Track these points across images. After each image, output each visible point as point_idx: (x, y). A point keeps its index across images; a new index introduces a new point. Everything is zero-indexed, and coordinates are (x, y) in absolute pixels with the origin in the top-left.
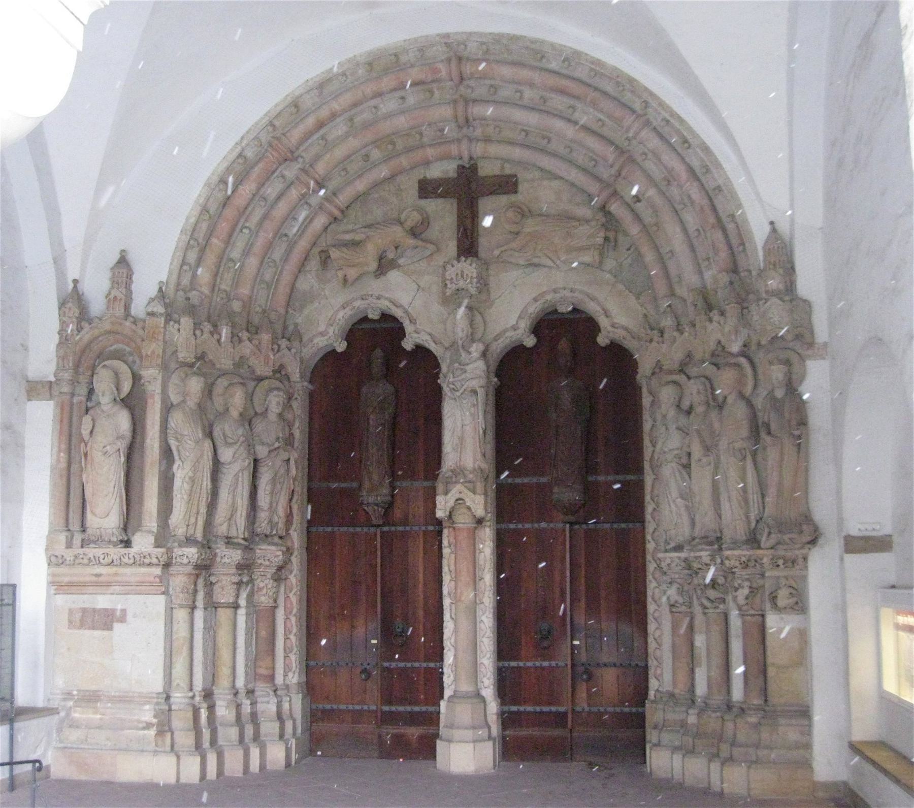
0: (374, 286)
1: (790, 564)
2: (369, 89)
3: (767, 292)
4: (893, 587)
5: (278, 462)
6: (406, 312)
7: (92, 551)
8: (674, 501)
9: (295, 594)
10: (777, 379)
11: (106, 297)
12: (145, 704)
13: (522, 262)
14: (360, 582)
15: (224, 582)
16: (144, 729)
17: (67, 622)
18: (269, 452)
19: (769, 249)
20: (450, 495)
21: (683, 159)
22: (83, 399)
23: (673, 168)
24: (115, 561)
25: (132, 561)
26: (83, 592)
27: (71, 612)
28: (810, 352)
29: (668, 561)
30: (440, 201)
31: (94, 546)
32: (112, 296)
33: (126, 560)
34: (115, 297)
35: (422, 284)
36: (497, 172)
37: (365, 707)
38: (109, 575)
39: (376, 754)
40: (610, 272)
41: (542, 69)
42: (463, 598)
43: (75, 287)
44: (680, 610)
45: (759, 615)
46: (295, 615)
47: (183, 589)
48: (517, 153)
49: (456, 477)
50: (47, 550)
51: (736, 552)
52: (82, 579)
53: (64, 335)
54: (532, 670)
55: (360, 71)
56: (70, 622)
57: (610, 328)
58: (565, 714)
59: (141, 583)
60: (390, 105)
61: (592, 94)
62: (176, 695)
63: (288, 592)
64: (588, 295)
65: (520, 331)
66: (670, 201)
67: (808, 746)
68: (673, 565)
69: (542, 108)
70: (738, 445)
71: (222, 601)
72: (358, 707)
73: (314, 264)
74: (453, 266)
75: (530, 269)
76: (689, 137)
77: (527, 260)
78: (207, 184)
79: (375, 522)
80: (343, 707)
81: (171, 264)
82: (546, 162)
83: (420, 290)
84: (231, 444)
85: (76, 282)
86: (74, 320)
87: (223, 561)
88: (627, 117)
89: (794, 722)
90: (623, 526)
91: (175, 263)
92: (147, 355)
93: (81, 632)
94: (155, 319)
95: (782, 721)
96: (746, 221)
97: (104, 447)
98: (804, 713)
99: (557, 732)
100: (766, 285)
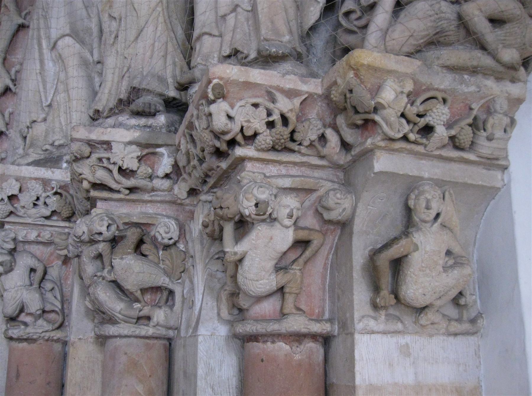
8: (54, 47)
45: (314, 337)
68: (26, 199)
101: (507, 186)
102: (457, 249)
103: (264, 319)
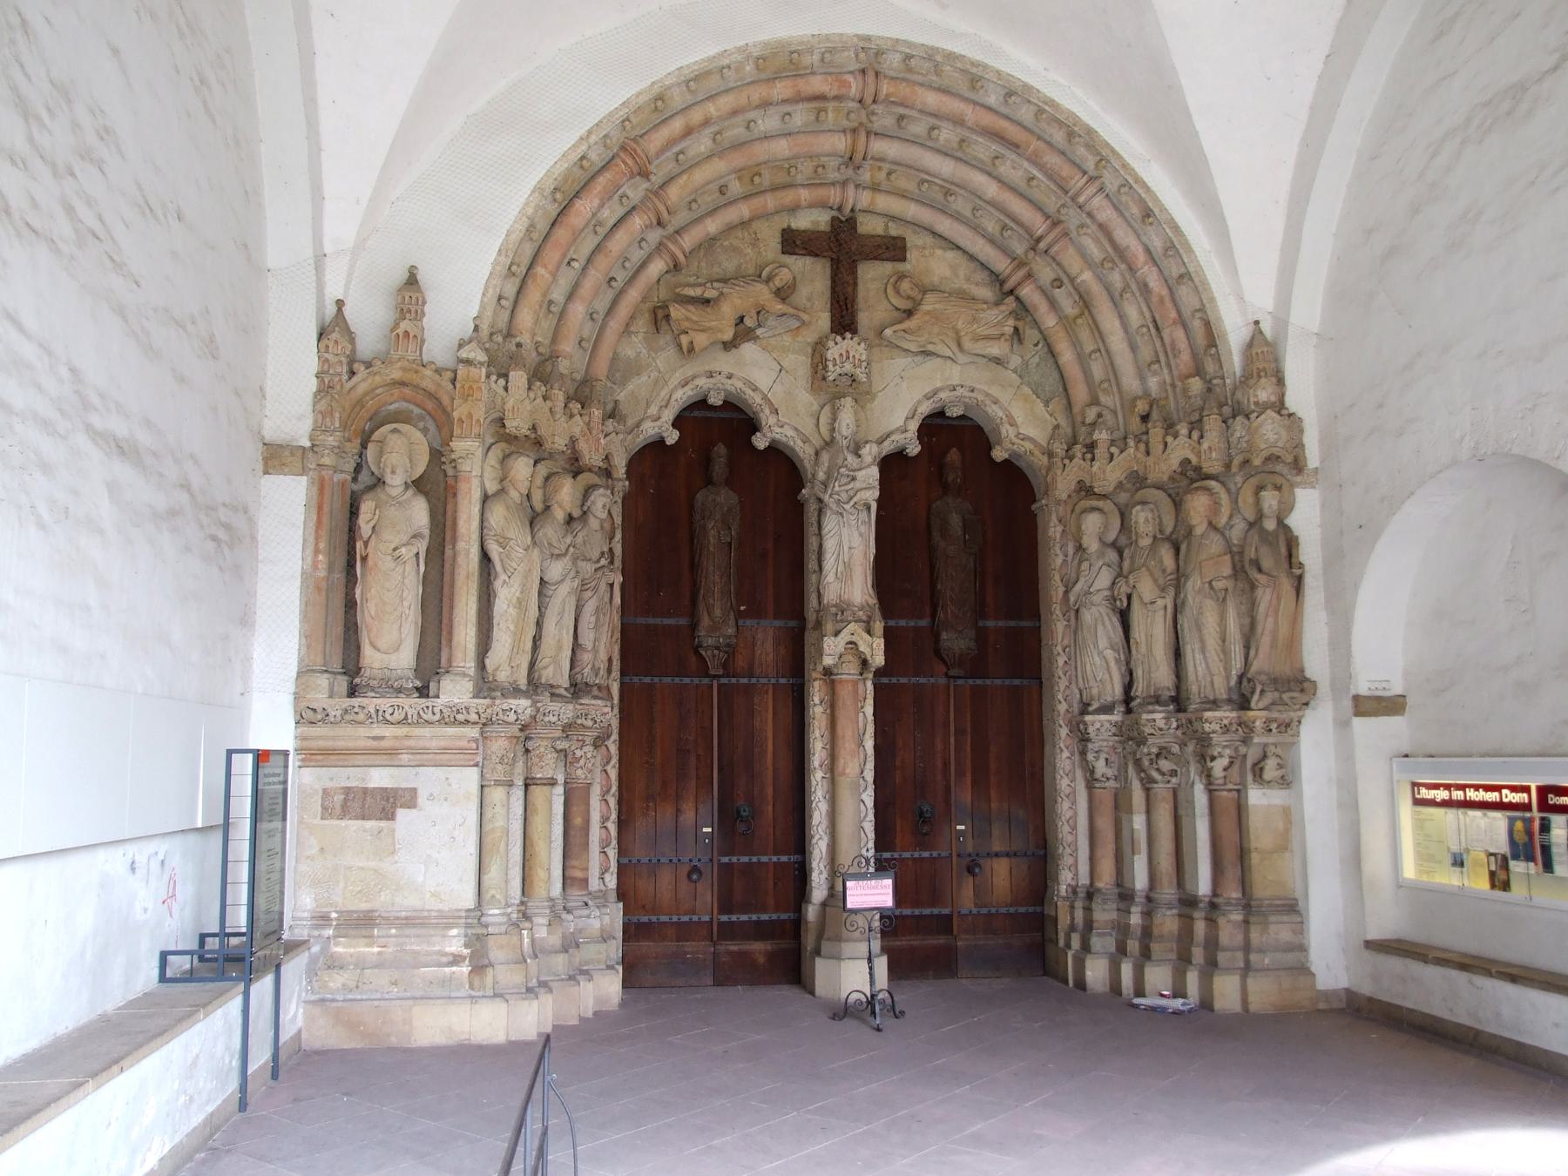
0: (723, 362)
1: (1283, 729)
2: (757, 94)
3: (1256, 403)
4: (1407, 756)
5: (603, 587)
6: (765, 397)
7: (371, 703)
9: (614, 767)
10: (1270, 506)
12: (449, 926)
13: (913, 347)
14: (688, 751)
15: (542, 749)
16: (451, 964)
17: (320, 809)
18: (595, 570)
19: (1257, 353)
20: (842, 635)
21: (1139, 237)
22: (349, 478)
23: (1128, 247)
24: (409, 717)
25: (437, 717)
26: (346, 763)
27: (326, 792)
28: (1298, 479)
29: (1098, 725)
30: (808, 260)
31: (373, 695)
32: (400, 331)
33: (428, 716)
34: (407, 333)
35: (785, 364)
36: (880, 231)
37: (695, 918)
38: (396, 738)
39: (710, 981)
40: (1015, 371)
41: (975, 103)
42: (847, 771)
43: (340, 310)
44: (1103, 785)
46: (613, 795)
48: (912, 210)
49: (843, 613)
50: (297, 697)
51: (1217, 714)
52: (351, 744)
53: (326, 381)
54: (910, 863)
55: (748, 68)
56: (324, 808)
57: (1015, 440)
58: (949, 918)
59: (445, 750)
60: (768, 122)
61: (1035, 144)
62: (491, 912)
64: (988, 395)
65: (909, 435)
66: (1108, 288)
67: (1302, 948)
68: (1103, 730)
69: (959, 154)
70: (1218, 585)
71: (538, 776)
72: (685, 918)
73: (642, 325)
74: (836, 344)
75: (919, 358)
76: (1156, 211)
77: (921, 346)
78: (538, 189)
79: (712, 672)
80: (664, 918)
81: (484, 294)
82: (945, 226)
83: (783, 372)
84: (559, 556)
85: (340, 304)
86: (344, 360)
87: (546, 719)
88: (1076, 178)
89: (1285, 918)
90: (1017, 682)
91: (489, 295)
92: (460, 420)
93: (343, 823)
94: (472, 369)
95: (1272, 918)
96: (1219, 319)
97: (395, 550)
98: (1292, 908)
99: (941, 940)
100: (1256, 396)
101: (1299, 741)
102: (1280, 762)
103: (1219, 785)
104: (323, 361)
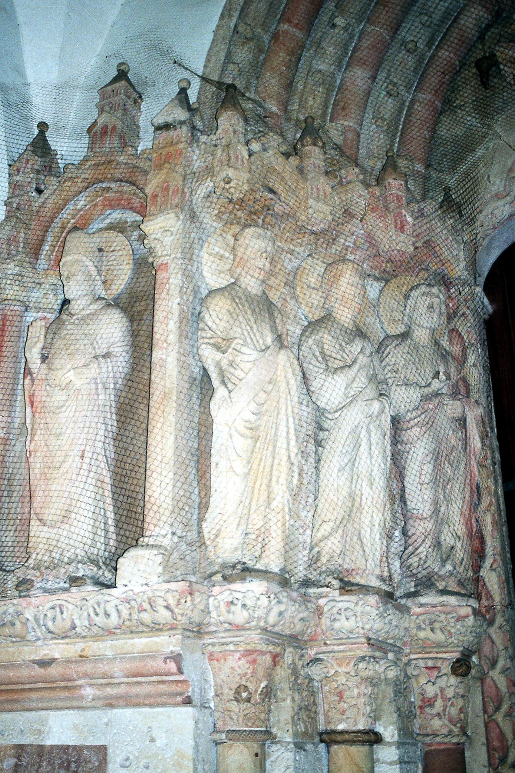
11: (89, 130)
43: (42, 133)
47: (237, 692)
63: (490, 710)
85: (43, 126)
87: (337, 625)
104: (14, 186)
